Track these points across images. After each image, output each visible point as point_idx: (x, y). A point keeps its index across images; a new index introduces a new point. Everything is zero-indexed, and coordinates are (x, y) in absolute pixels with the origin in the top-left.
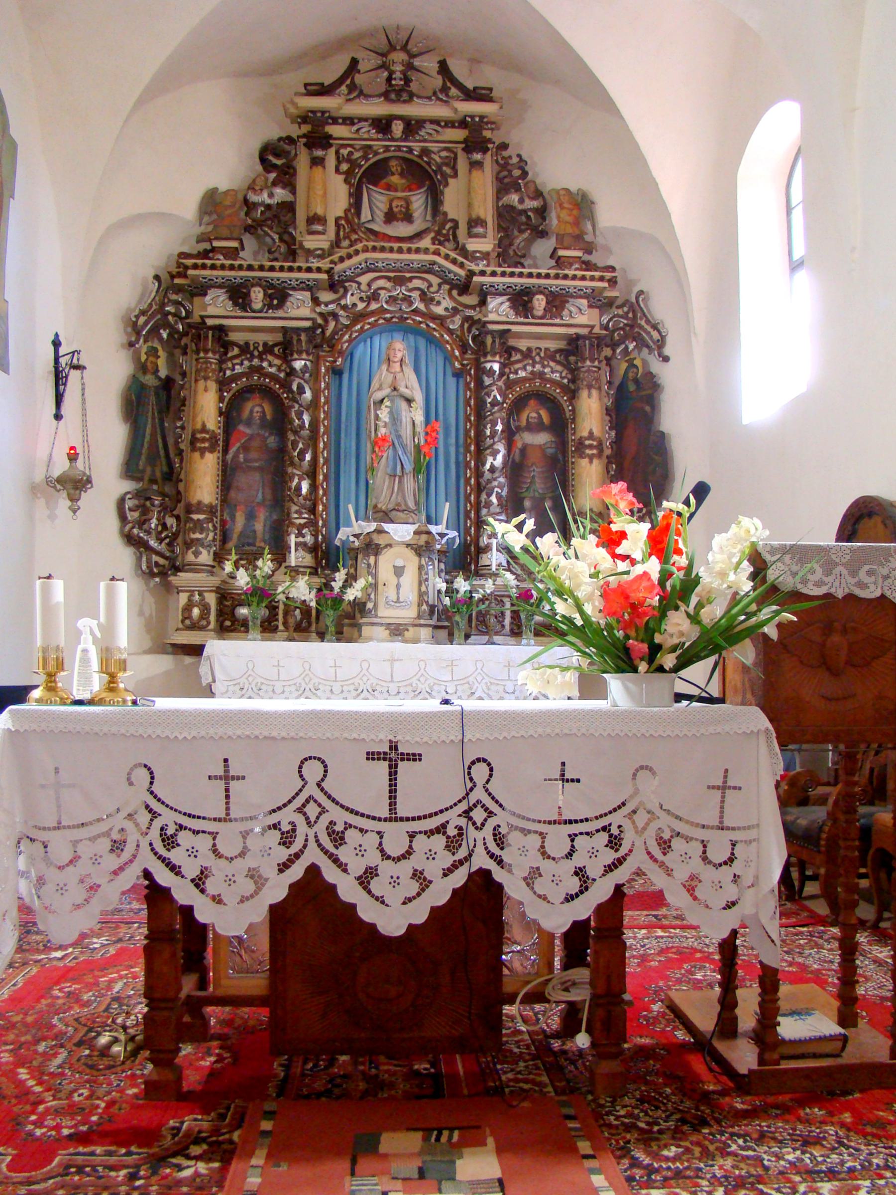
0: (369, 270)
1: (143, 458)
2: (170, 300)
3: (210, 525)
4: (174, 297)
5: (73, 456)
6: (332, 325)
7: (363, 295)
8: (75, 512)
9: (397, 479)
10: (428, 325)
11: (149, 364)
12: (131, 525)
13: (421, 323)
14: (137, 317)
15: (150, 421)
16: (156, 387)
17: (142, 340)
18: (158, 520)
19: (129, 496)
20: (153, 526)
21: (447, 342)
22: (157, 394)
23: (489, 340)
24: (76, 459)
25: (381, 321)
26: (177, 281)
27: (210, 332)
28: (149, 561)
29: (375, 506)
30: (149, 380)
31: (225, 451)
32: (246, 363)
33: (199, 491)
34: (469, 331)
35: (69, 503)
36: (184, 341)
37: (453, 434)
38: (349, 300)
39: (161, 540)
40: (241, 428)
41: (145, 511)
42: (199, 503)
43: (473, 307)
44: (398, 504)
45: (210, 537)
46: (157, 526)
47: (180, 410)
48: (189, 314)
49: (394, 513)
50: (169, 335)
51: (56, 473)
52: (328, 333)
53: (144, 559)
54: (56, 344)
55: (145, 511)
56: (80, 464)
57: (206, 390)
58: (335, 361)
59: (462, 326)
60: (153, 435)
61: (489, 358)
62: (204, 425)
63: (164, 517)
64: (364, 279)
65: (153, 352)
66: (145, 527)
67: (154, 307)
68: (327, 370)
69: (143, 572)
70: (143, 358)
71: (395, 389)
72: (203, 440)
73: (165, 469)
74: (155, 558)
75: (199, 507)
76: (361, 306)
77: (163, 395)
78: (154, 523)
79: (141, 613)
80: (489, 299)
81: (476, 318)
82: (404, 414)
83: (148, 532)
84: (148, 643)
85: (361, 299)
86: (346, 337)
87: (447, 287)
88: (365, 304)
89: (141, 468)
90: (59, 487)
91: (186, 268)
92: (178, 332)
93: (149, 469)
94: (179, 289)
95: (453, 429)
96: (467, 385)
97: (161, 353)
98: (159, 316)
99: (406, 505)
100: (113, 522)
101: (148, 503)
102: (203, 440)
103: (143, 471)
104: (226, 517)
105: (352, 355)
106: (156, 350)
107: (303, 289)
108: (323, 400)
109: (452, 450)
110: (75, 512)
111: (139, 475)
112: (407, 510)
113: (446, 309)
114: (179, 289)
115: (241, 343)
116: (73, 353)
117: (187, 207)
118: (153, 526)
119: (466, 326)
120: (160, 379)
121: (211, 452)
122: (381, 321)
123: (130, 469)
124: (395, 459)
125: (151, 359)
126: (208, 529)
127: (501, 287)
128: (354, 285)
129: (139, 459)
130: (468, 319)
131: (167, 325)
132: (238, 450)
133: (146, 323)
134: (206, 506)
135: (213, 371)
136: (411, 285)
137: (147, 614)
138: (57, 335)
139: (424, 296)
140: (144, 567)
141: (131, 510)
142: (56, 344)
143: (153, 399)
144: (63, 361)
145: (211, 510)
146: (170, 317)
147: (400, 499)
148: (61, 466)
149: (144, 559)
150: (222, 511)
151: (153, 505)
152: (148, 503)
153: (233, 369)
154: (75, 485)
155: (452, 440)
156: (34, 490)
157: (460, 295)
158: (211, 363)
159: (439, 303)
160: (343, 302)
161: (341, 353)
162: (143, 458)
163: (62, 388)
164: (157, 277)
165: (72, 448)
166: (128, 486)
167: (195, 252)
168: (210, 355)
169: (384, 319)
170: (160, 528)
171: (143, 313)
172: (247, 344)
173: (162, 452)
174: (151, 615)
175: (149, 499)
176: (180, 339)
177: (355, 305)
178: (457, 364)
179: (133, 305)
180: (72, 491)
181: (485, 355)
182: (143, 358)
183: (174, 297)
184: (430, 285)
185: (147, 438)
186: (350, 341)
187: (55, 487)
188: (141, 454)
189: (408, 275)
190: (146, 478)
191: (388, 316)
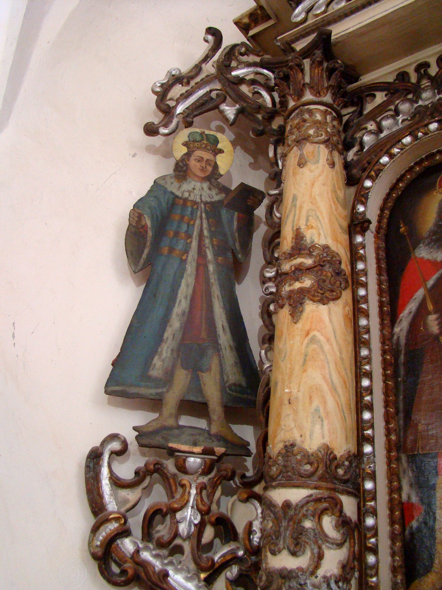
3: (328, 523)
11: (193, 163)
12: (112, 526)
14: (166, 88)
15: (190, 268)
16: (213, 209)
19: (116, 446)
27: (307, 63)
31: (390, 315)
32: (405, 107)
33: (287, 410)
40: (423, 253)
42: (290, 448)
45: (333, 560)
57: (301, 164)
60: (201, 296)
62: (298, 236)
66: (162, 530)
72: (299, 272)
73: (233, 375)
75: (293, 466)
77: (231, 220)
78: (189, 517)
92: (260, 108)
93: (182, 378)
97: (224, 141)
100: (76, 520)
101: (170, 465)
102: (299, 272)
104: (407, 493)
111: (151, 392)
115: (391, 79)
118: (183, 528)
120: (224, 189)
121: (324, 301)
123: (125, 380)
125: (199, 153)
126: (321, 535)
129: (154, 352)
131: (240, 97)
132: (422, 305)
134: (308, 458)
135: (318, 125)
145: (340, 475)
146: (244, 89)
150: (393, 475)
151: (182, 468)
153: (380, 130)
158: (310, 112)
166: (126, 422)
168: (308, 96)
171: (177, 79)
172: (403, 76)
173: (225, 339)
175: (172, 452)
183: (252, 58)
185: (182, 305)
188: (159, 339)
190: (172, 398)
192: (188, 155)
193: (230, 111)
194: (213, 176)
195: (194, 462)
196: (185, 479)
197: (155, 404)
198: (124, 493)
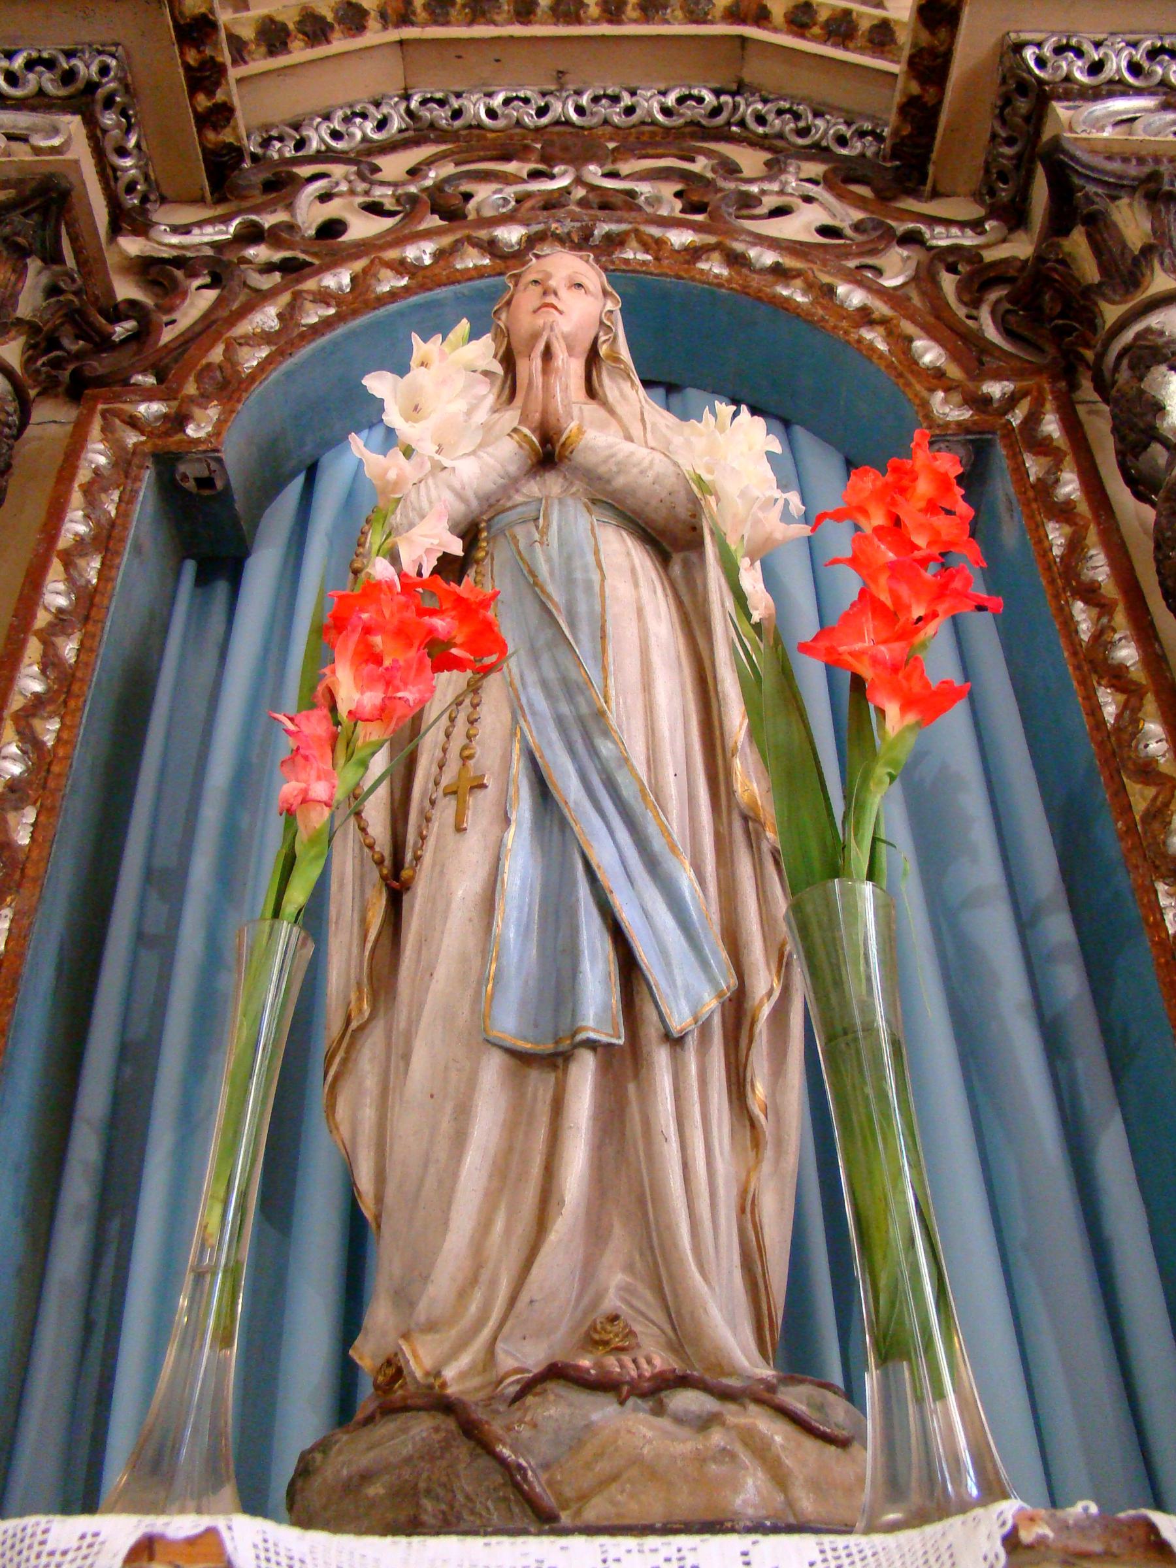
0: (419, 132)
6: (199, 301)
7: (383, 194)
9: (584, 1075)
10: (736, 260)
13: (695, 253)
21: (865, 316)
23: (1132, 223)
25: (472, 259)
29: (394, 1370)
34: (976, 304)
37: (982, 834)
38: (309, 213)
43: (976, 226)
44: (603, 1333)
49: (558, 1409)
52: (167, 336)
58: (179, 420)
59: (924, 278)
61: (1161, 282)
64: (394, 166)
68: (124, 463)
71: (548, 453)
76: (362, 227)
80: (1061, 110)
81: (990, 256)
82: (619, 589)
85: (374, 208)
86: (267, 317)
87: (815, 169)
88: (388, 223)
95: (973, 802)
96: (1041, 500)
99: (682, 1330)
105: (312, 472)
107: (40, 102)
108: (56, 595)
109: (994, 932)
112: (691, 1373)
113: (824, 231)
119: (948, 282)
122: (472, 259)
124: (555, 918)
127: (1117, 65)
128: (338, 170)
130: (951, 258)
136: (625, 168)
139: (696, 199)
147: (616, 1284)
155: (982, 869)
157: (884, 197)
159: (780, 212)
160: (268, 221)
161: (229, 387)
169: (491, 247)
177: (332, 229)
178: (947, 409)
181: (1125, 272)
184: (730, 169)
186: (286, 340)
189: (611, 145)
191: (511, 235)
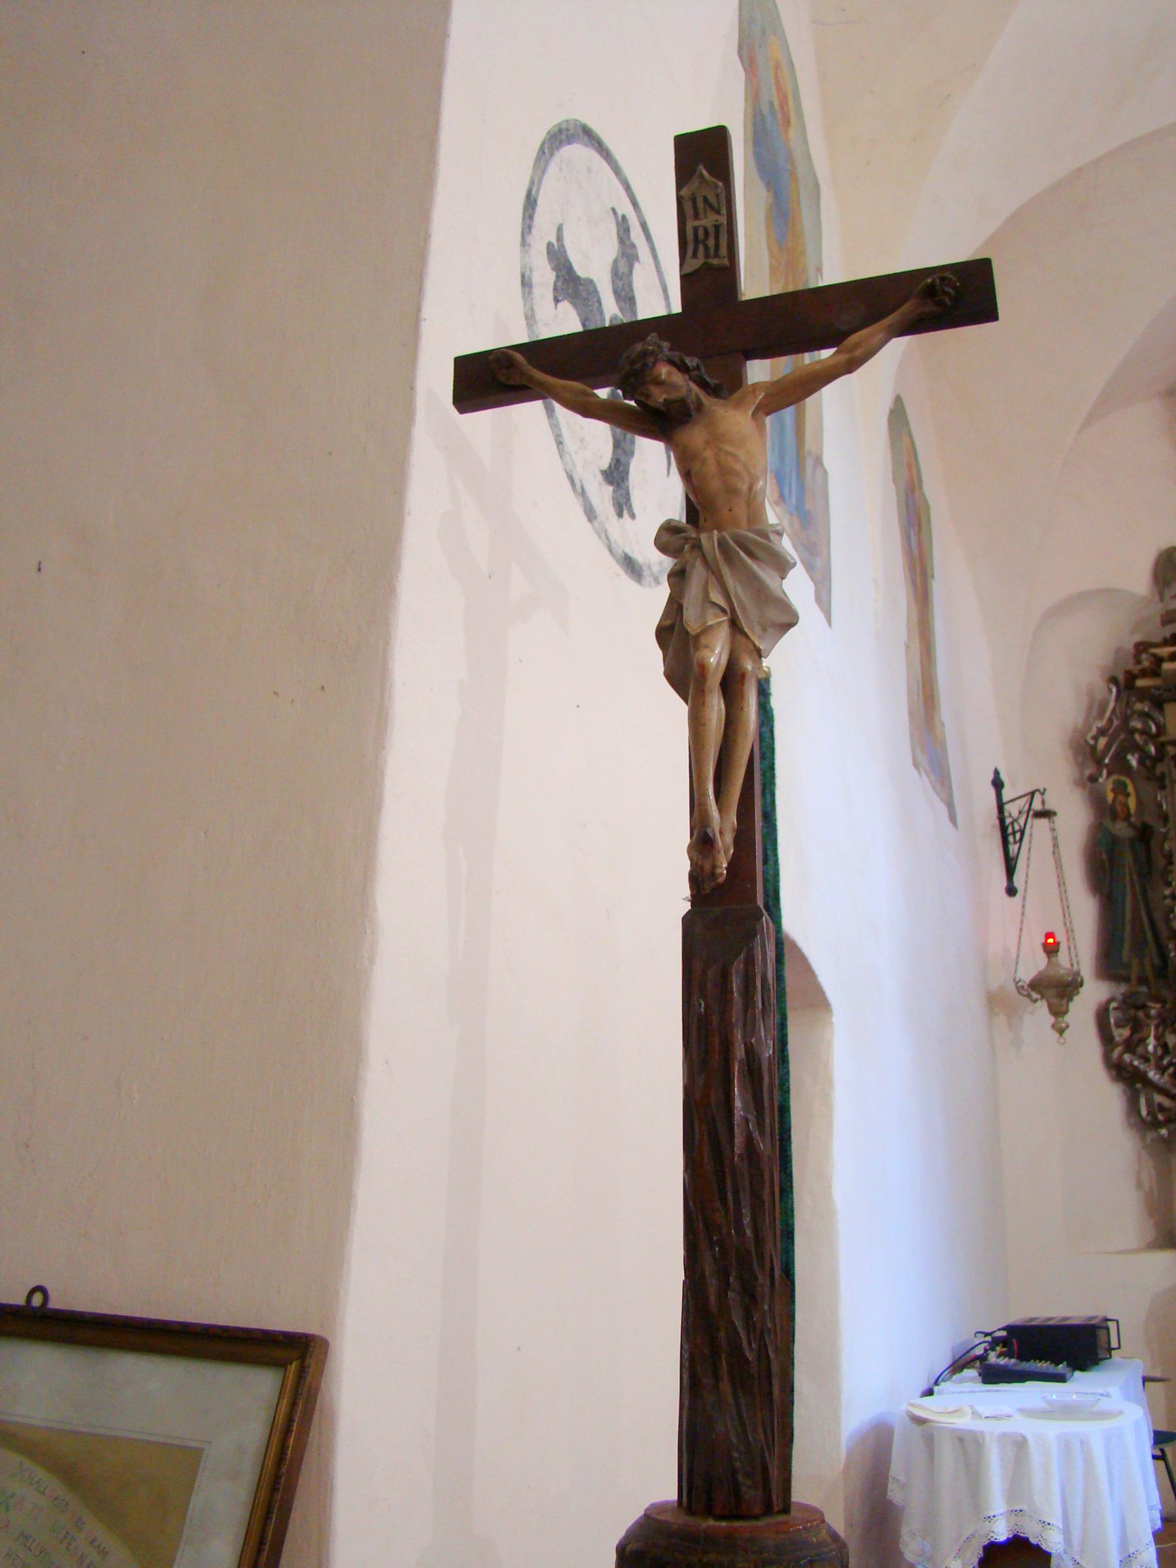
1: (1127, 945)
2: (1134, 712)
4: (1138, 706)
5: (1051, 950)
8: (1061, 1032)
14: (1095, 738)
16: (1132, 840)
17: (1105, 772)
18: (1157, 1038)
19: (1113, 1005)
20: (1150, 1048)
22: (1133, 848)
24: (1057, 951)
26: (1140, 683)
28: (1150, 1104)
30: (1121, 829)
35: (1052, 1019)
36: (1160, 769)
39: (1162, 1070)
41: (1137, 1026)
46: (1155, 1047)
47: (1166, 872)
48: (1161, 729)
50: (1141, 762)
51: (1027, 974)
53: (1143, 1101)
54: (998, 784)
55: (1137, 1026)
56: (1063, 957)
60: (1135, 909)
63: (1163, 1035)
65: (1120, 789)
66: (1140, 1050)
67: (1116, 723)
69: (1143, 1120)
70: (1110, 796)
73: (1157, 961)
74: (1158, 1098)
79: (1139, 1185)
83: (1145, 1059)
84: (1150, 1234)
89: (1125, 960)
90: (1035, 995)
91: (1159, 660)
92: (1149, 756)
93: (1135, 962)
94: (1143, 695)
98: (1123, 736)
103: (1128, 966)
106: (1125, 786)
110: (1061, 1032)
114: (1143, 695)
116: (1032, 794)
117: (1138, 580)
118: (1150, 1048)
123: (1110, 963)
125: (1120, 798)
133: (1108, 746)
137: (1146, 1185)
138: (997, 773)
140: (1144, 1112)
141: (1118, 1026)
142: (998, 784)
143: (1128, 858)
144: (1012, 809)
146: (1137, 737)
148: (1033, 964)
149: (1143, 1101)
151: (1148, 1016)
152: (1141, 1014)
154: (1056, 990)
156: (995, 1002)
162: (1127, 945)
163: (1013, 849)
164: (1113, 680)
165: (1049, 935)
167: (1159, 639)
170: (1160, 1052)
171: (1102, 732)
173: (1149, 936)
174: (1151, 1187)
176: (1153, 767)
179: (1080, 723)
180: (1055, 1001)
182: (1110, 796)
183: (1138, 706)
187: (1029, 996)
188: (1122, 939)
192: (1114, 800)
193: (1133, 761)
194: (1127, 818)
195: (1153, 1012)
196: (1148, 1021)
197: (1126, 979)
198: (1120, 1031)
